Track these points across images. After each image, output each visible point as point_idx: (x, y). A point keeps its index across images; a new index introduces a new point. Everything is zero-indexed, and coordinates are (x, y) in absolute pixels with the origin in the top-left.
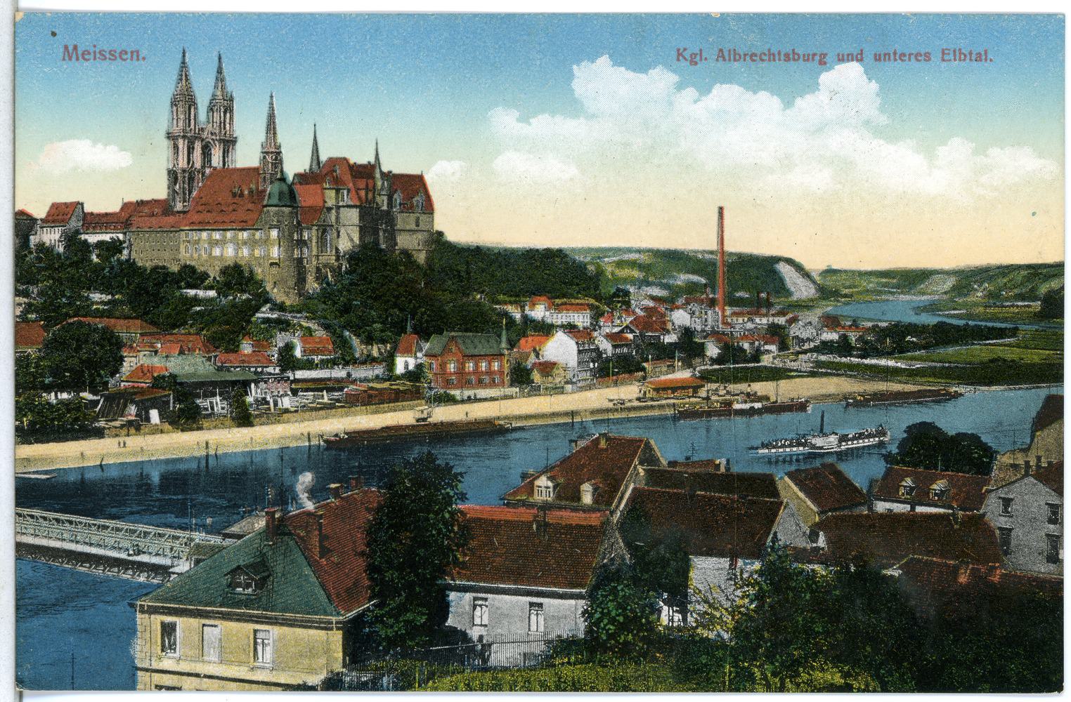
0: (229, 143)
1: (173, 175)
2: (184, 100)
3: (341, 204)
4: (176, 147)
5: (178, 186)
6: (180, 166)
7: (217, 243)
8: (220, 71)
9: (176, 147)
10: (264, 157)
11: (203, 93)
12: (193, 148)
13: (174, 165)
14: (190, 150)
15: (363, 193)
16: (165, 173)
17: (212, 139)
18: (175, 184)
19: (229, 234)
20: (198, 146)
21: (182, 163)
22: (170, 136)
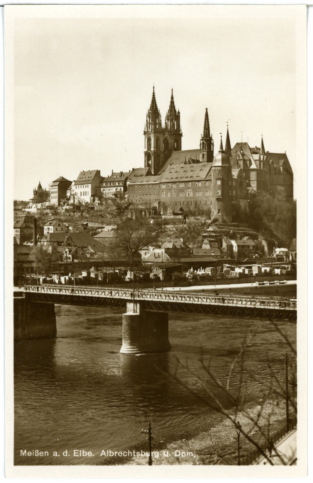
1: (148, 155)
2: (154, 112)
4: (149, 140)
5: (151, 161)
6: (152, 149)
7: (182, 190)
8: (172, 98)
10: (203, 143)
11: (163, 110)
12: (159, 140)
13: (149, 150)
14: (157, 140)
15: (258, 162)
17: (169, 135)
21: (152, 149)
22: (145, 133)
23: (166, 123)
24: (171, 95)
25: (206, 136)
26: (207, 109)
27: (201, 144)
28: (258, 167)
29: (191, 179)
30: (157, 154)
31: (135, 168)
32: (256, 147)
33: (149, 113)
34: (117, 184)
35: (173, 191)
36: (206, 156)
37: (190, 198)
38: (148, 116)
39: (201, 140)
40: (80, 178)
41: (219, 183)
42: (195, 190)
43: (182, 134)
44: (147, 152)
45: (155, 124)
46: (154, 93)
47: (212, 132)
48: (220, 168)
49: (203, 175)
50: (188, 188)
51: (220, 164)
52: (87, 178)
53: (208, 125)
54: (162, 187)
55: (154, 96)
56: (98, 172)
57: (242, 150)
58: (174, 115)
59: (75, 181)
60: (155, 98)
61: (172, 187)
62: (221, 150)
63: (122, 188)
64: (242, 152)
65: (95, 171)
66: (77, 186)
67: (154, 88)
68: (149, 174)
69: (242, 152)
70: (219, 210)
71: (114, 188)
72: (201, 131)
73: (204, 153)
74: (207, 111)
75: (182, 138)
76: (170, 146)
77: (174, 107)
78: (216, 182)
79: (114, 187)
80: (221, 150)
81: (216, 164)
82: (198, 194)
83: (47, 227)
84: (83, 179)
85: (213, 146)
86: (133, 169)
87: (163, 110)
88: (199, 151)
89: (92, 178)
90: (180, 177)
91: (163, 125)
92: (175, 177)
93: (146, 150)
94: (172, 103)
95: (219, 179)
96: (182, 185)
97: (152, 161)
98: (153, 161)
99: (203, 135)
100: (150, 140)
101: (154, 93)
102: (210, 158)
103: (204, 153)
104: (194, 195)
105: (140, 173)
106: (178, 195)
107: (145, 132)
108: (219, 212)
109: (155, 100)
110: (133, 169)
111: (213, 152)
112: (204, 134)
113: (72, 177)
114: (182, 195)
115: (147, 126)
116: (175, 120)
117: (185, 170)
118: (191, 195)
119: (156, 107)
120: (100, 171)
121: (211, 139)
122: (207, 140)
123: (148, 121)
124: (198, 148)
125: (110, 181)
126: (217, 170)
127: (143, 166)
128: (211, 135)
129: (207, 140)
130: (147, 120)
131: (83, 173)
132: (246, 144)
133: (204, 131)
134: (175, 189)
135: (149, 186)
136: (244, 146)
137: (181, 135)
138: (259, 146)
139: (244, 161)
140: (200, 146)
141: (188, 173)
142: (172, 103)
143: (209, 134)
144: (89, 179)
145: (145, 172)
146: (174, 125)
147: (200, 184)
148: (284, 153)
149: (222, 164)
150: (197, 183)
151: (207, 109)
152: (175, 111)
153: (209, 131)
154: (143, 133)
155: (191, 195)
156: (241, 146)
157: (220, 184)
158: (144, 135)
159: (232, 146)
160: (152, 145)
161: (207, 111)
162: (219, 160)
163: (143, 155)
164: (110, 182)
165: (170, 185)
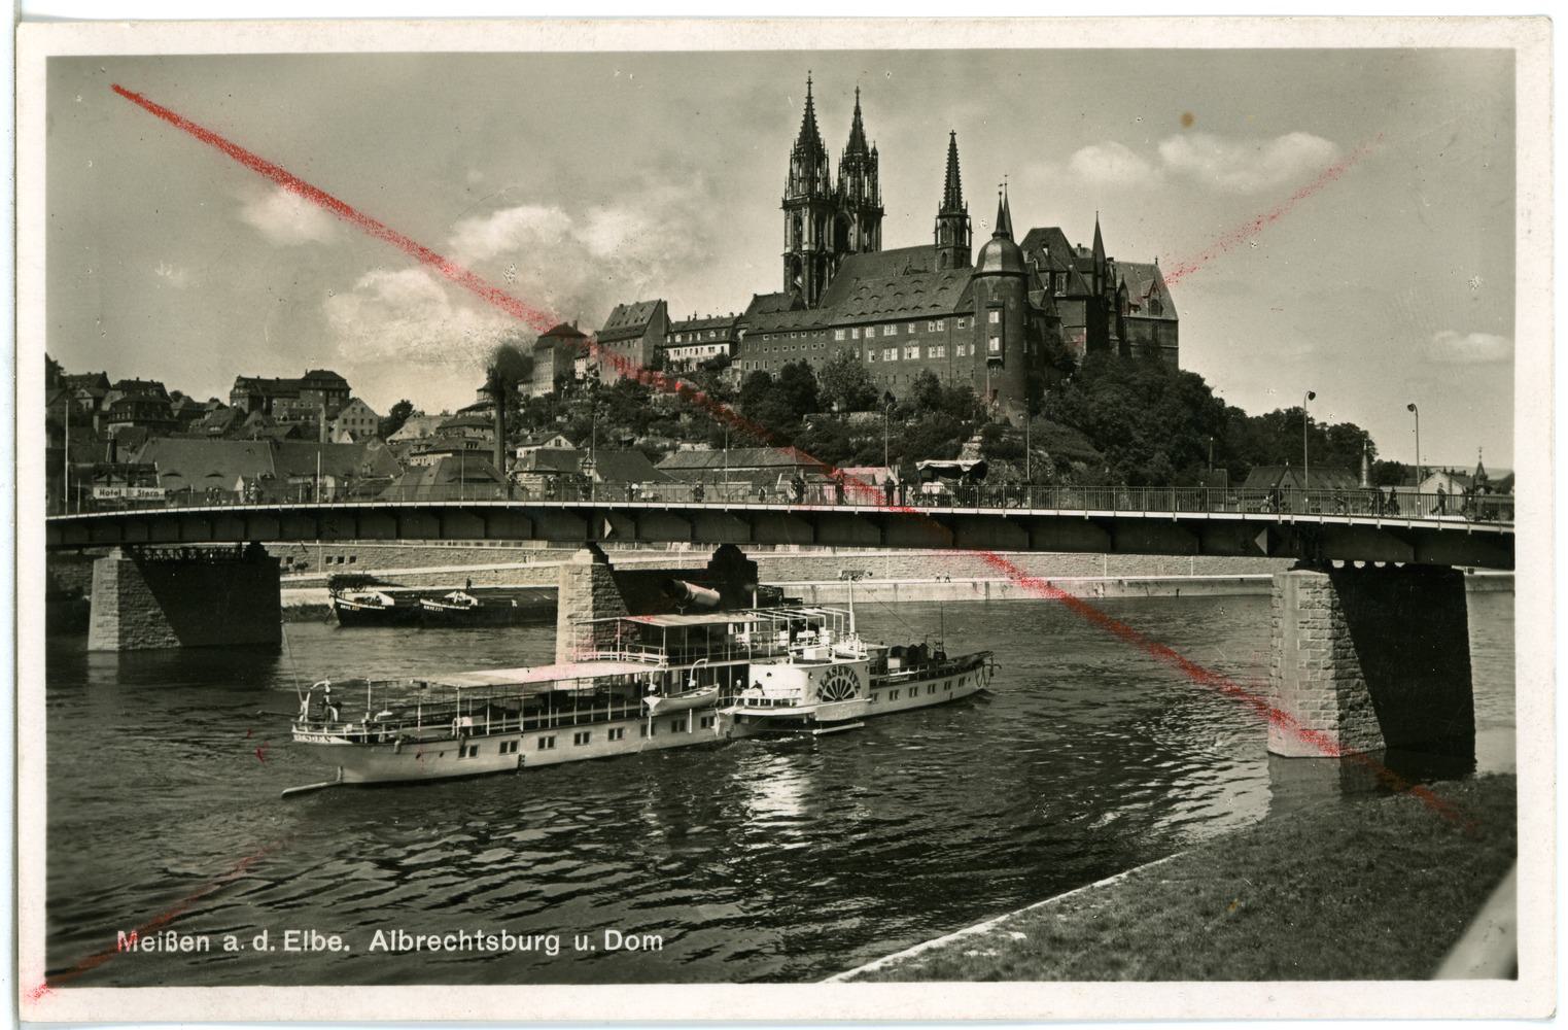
0: (872, 216)
1: (793, 263)
2: (810, 149)
3: (1057, 294)
4: (798, 222)
5: (799, 279)
6: (805, 248)
7: (890, 343)
9: (798, 222)
10: (944, 225)
11: (835, 145)
13: (795, 247)
14: (819, 223)
15: (1089, 279)
16: (782, 260)
18: (795, 277)
19: (911, 328)
20: (830, 225)
22: (786, 206)
23: (840, 180)
24: (854, 104)
25: (953, 205)
26: (953, 134)
27: (937, 229)
28: (1091, 287)
29: (917, 314)
30: (818, 260)
31: (760, 293)
32: (1079, 245)
34: (713, 335)
35: (865, 347)
36: (950, 260)
37: (913, 363)
38: (797, 157)
39: (940, 217)
40: (611, 323)
41: (995, 317)
43: (882, 209)
44: (790, 254)
45: (812, 180)
46: (810, 98)
47: (966, 196)
48: (999, 278)
49: (950, 301)
50: (910, 337)
51: (998, 268)
52: (631, 323)
53: (958, 176)
54: (837, 338)
55: (810, 104)
56: (661, 306)
57: (1046, 246)
58: (861, 159)
60: (812, 110)
61: (862, 335)
62: (1000, 231)
63: (727, 347)
64: (1045, 250)
65: (653, 302)
66: (606, 345)
67: (810, 83)
68: (797, 306)
69: (1045, 250)
70: (995, 392)
71: (706, 348)
72: (939, 196)
73: (946, 251)
74: (953, 139)
75: (883, 219)
76: (853, 241)
77: (863, 137)
78: (988, 316)
79: (705, 344)
80: (1000, 231)
83: (525, 449)
84: (623, 325)
85: (970, 233)
86: (756, 297)
87: (835, 145)
88: (935, 248)
89: (645, 322)
90: (886, 308)
91: (834, 184)
92: (872, 307)
93: (788, 250)
94: (857, 126)
95: (994, 307)
96: (890, 331)
97: (803, 280)
98: (806, 278)
99: (942, 205)
100: (801, 224)
101: (810, 98)
103: (946, 251)
104: (924, 353)
105: (775, 305)
107: (785, 202)
108: (995, 397)
109: (813, 116)
110: (756, 297)
111: (969, 250)
112: (947, 202)
115: (791, 185)
116: (867, 172)
117: (898, 290)
118: (916, 353)
119: (816, 134)
120: (665, 303)
121: (964, 216)
122: (954, 218)
123: (795, 171)
124: (933, 242)
125: (695, 330)
126: (991, 282)
127: (781, 290)
128: (964, 200)
129: (954, 218)
130: (791, 170)
131: (621, 310)
132: (1057, 231)
133: (947, 194)
134: (870, 341)
135: (799, 337)
136: (1051, 236)
137: (881, 212)
138: (1089, 244)
139: (1053, 274)
140: (936, 233)
141: (907, 298)
142: (857, 126)
143: (960, 202)
144: (639, 323)
145: (786, 305)
146: (861, 185)
147: (940, 323)
148: (1153, 262)
149: (1003, 265)
150: (930, 324)
151: (953, 134)
152: (865, 148)
153: (959, 193)
154: (781, 205)
155: (916, 353)
156: (1047, 238)
157: (997, 320)
158: (783, 212)
159: (1019, 238)
160: (806, 238)
161: (953, 139)
162: (997, 256)
163: (781, 261)
164: (695, 331)
165: (855, 333)
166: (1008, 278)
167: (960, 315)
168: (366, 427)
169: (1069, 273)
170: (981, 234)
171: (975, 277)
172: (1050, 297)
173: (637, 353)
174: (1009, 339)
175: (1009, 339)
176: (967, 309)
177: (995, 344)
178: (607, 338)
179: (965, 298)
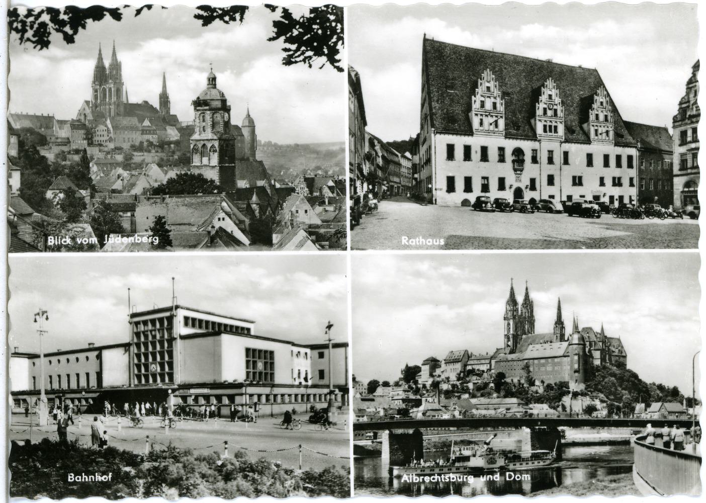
7: (543, 365)
15: (601, 344)
19: (550, 360)
33: (508, 302)
36: (559, 338)
41: (576, 358)
42: (555, 364)
59: (445, 360)
63: (489, 365)
68: (512, 352)
70: (576, 381)
81: (574, 342)
82: (556, 368)
84: (453, 358)
89: (461, 357)
95: (576, 354)
96: (543, 361)
102: (562, 338)
106: (539, 369)
113: (441, 357)
114: (543, 369)
121: (562, 323)
134: (536, 364)
165: (531, 361)
166: (580, 346)
167: (565, 356)
168: (364, 391)
169: (595, 342)
170: (569, 330)
171: (570, 345)
172: (590, 351)
173: (458, 367)
174: (581, 364)
175: (581, 364)
176: (567, 354)
177: (576, 366)
178: (449, 362)
179: (566, 351)
